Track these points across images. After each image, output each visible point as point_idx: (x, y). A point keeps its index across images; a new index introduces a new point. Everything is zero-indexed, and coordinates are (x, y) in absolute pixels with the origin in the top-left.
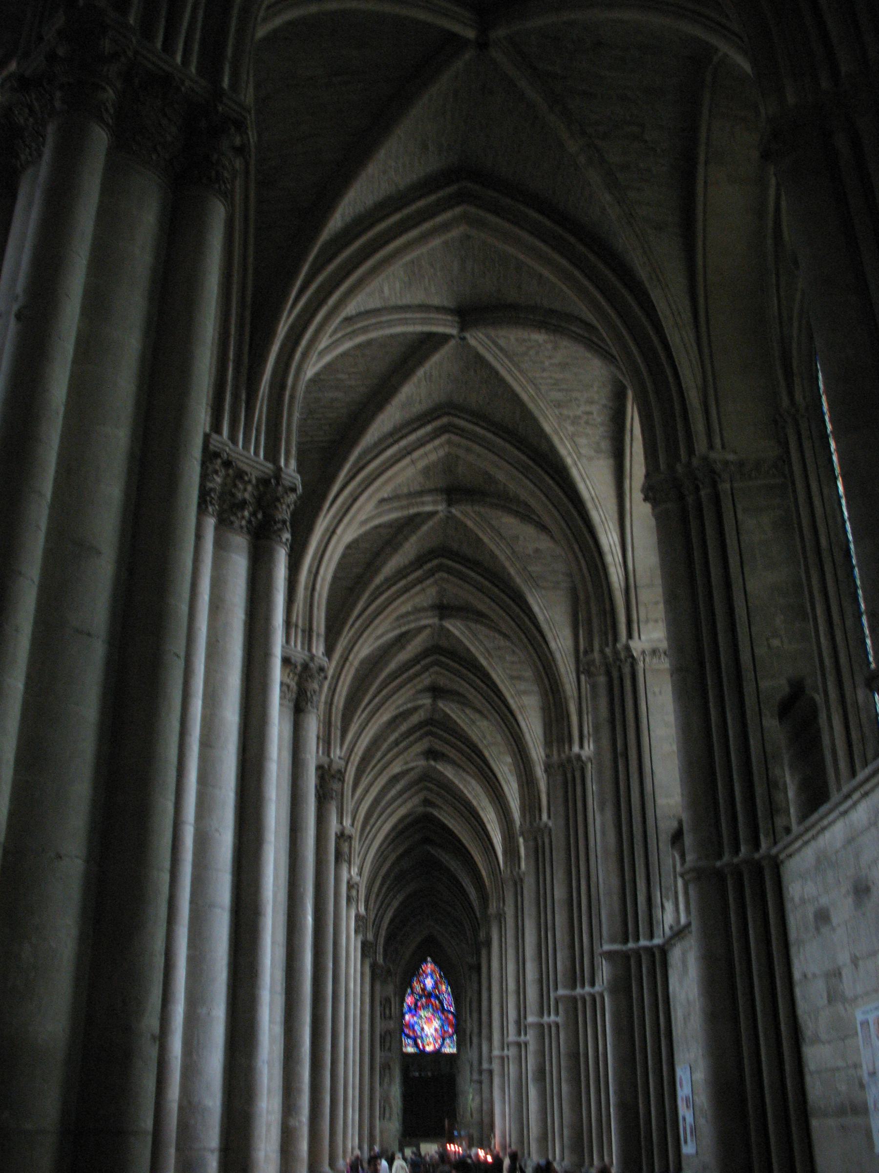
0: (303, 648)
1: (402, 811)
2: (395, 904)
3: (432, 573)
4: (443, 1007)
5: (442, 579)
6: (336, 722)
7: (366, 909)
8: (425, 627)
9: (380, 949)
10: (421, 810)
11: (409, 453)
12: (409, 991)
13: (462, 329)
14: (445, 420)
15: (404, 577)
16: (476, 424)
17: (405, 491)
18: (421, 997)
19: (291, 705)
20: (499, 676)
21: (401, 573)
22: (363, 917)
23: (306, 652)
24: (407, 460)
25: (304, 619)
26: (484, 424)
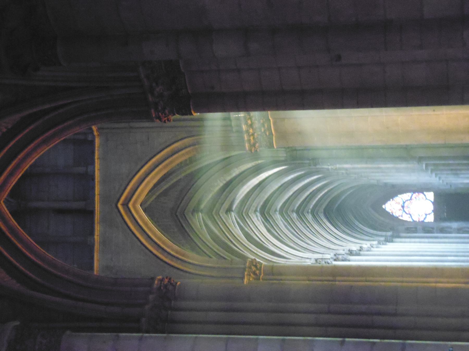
2: (360, 226)
3: (270, 216)
4: (409, 200)
7: (373, 241)
9: (384, 233)
12: (400, 218)
13: (232, 211)
14: (244, 215)
18: (404, 211)
22: (378, 242)
24: (258, 227)
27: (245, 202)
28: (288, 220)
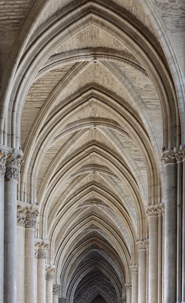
0: (8, 146)
1: (80, 231)
5: (92, 101)
6: (34, 185)
8: (86, 130)
10: (91, 230)
11: (68, 26)
15: (72, 101)
16: (107, 8)
17: (68, 49)
19: (3, 176)
20: (127, 157)
21: (70, 99)
23: (10, 147)
24: (67, 30)
25: (8, 127)
26: (112, 8)
27: (110, 7)
28: (84, 152)
